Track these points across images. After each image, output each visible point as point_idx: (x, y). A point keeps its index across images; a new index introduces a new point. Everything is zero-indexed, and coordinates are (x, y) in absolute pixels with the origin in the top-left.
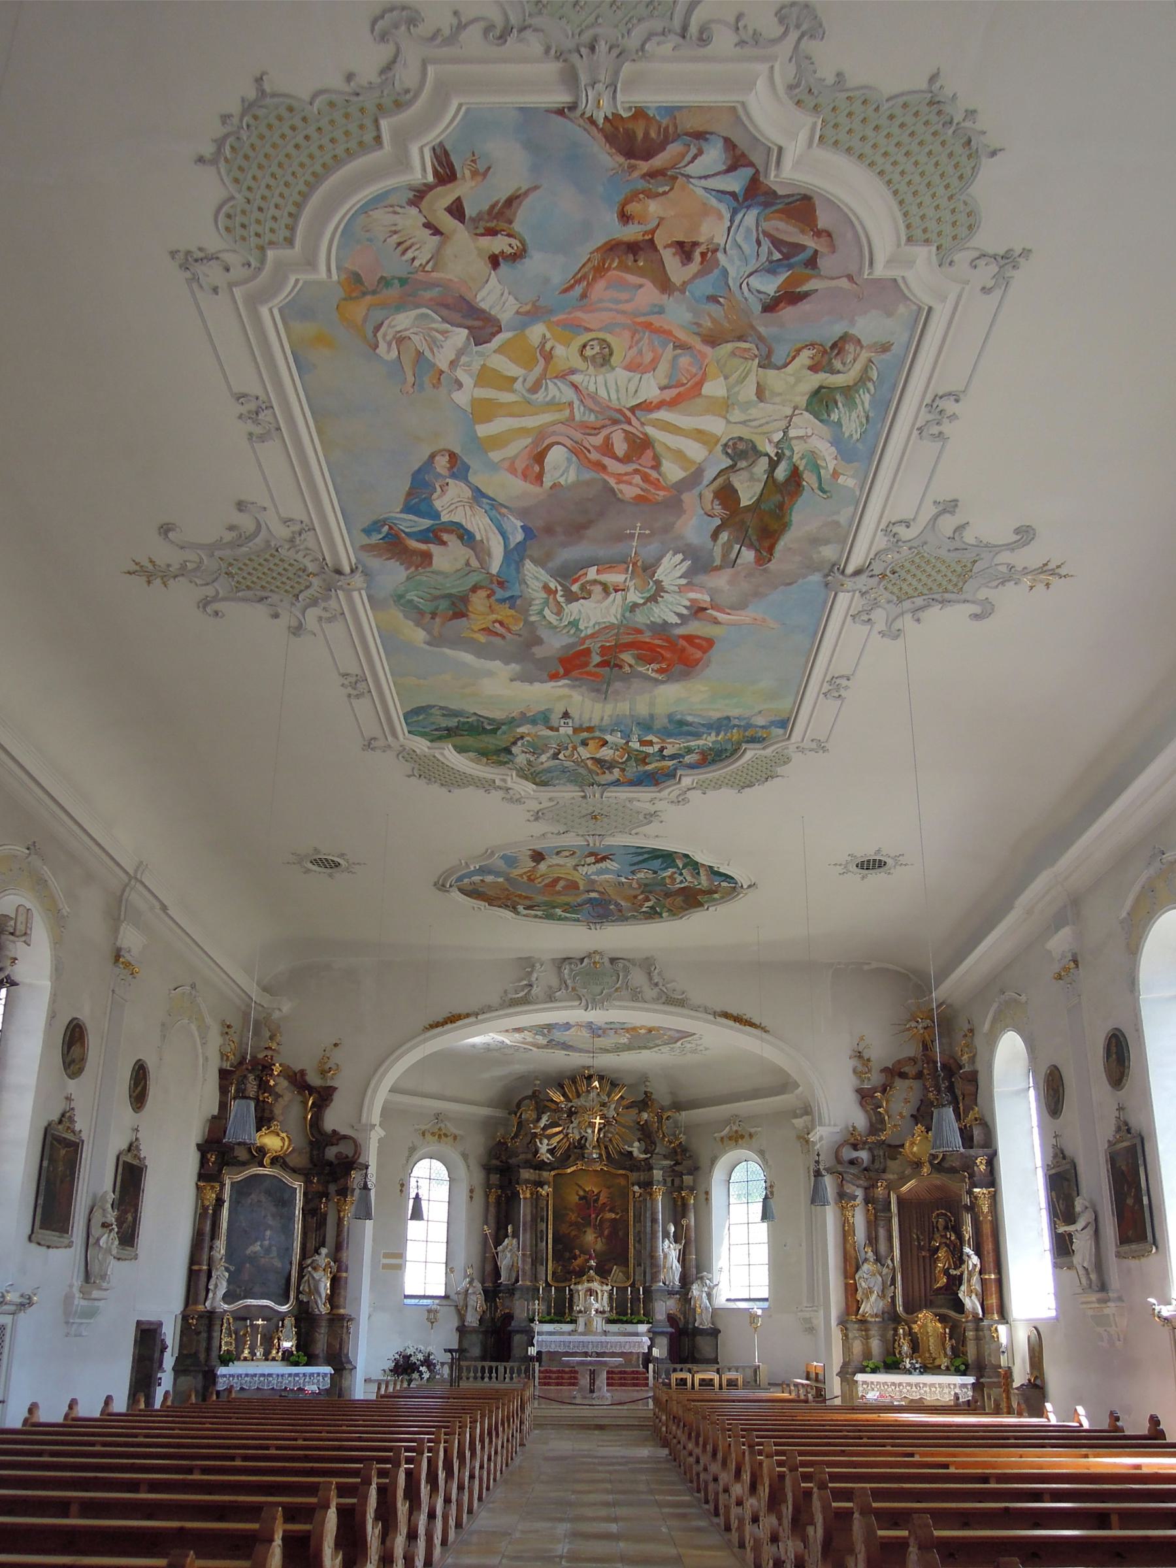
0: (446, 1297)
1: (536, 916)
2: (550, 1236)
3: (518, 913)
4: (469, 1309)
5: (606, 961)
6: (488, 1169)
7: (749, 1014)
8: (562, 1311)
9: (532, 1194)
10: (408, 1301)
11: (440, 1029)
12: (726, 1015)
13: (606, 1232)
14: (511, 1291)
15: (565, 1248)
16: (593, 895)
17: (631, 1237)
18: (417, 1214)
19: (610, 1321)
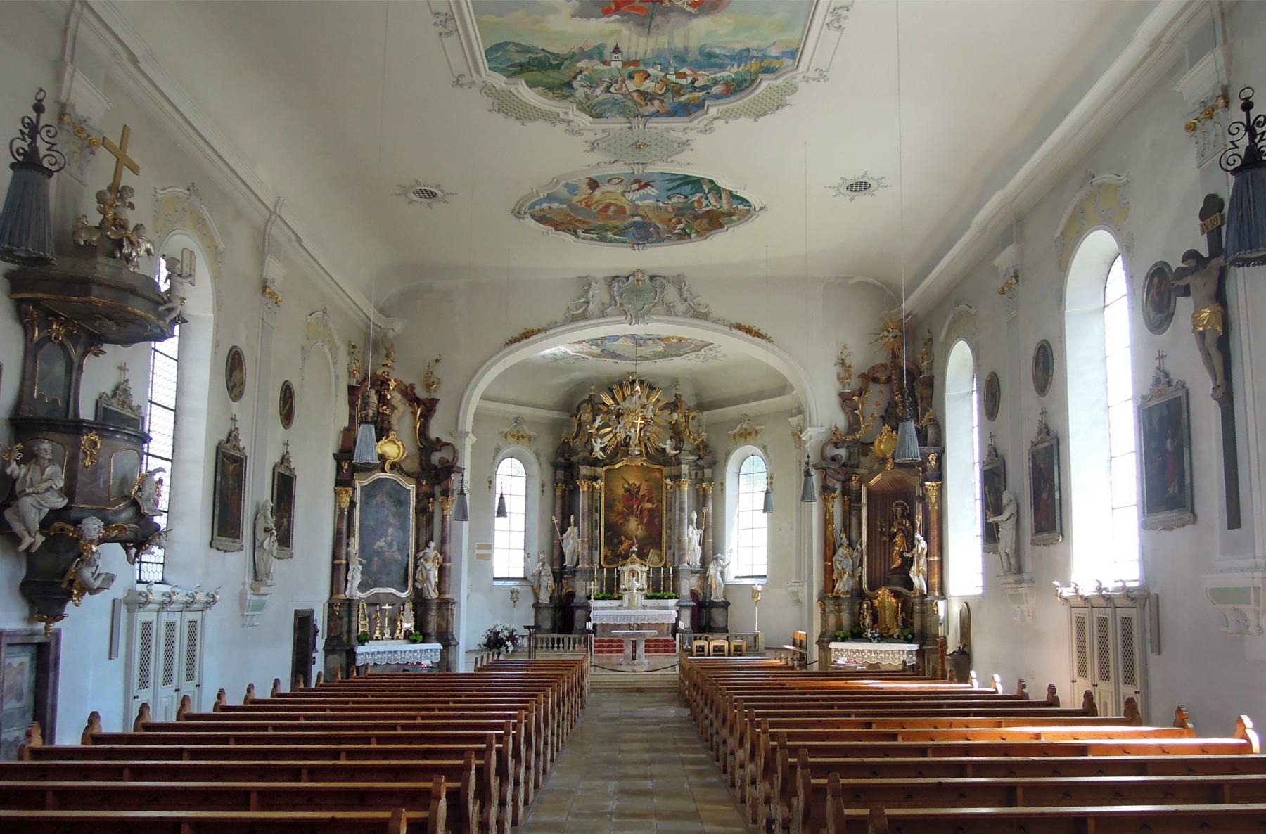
0: (525, 579)
1: (592, 239)
3: (578, 237)
5: (647, 278)
7: (759, 326)
8: (611, 590)
10: (496, 583)
11: (517, 344)
12: (739, 327)
14: (573, 573)
15: (614, 534)
16: (637, 219)
18: (502, 512)
19: (648, 597)
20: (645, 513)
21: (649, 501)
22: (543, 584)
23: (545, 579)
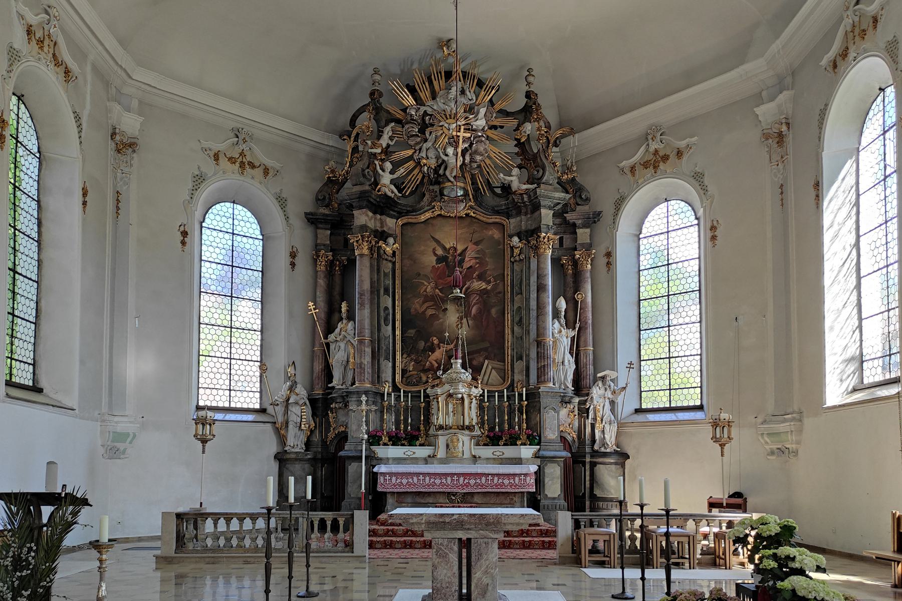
0: (262, 411)
2: (398, 316)
4: (291, 426)
6: (312, 220)
9: (371, 249)
13: (474, 310)
15: (419, 335)
17: (508, 317)
20: (474, 299)
21: (481, 278)
22: (294, 418)
23: (295, 410)
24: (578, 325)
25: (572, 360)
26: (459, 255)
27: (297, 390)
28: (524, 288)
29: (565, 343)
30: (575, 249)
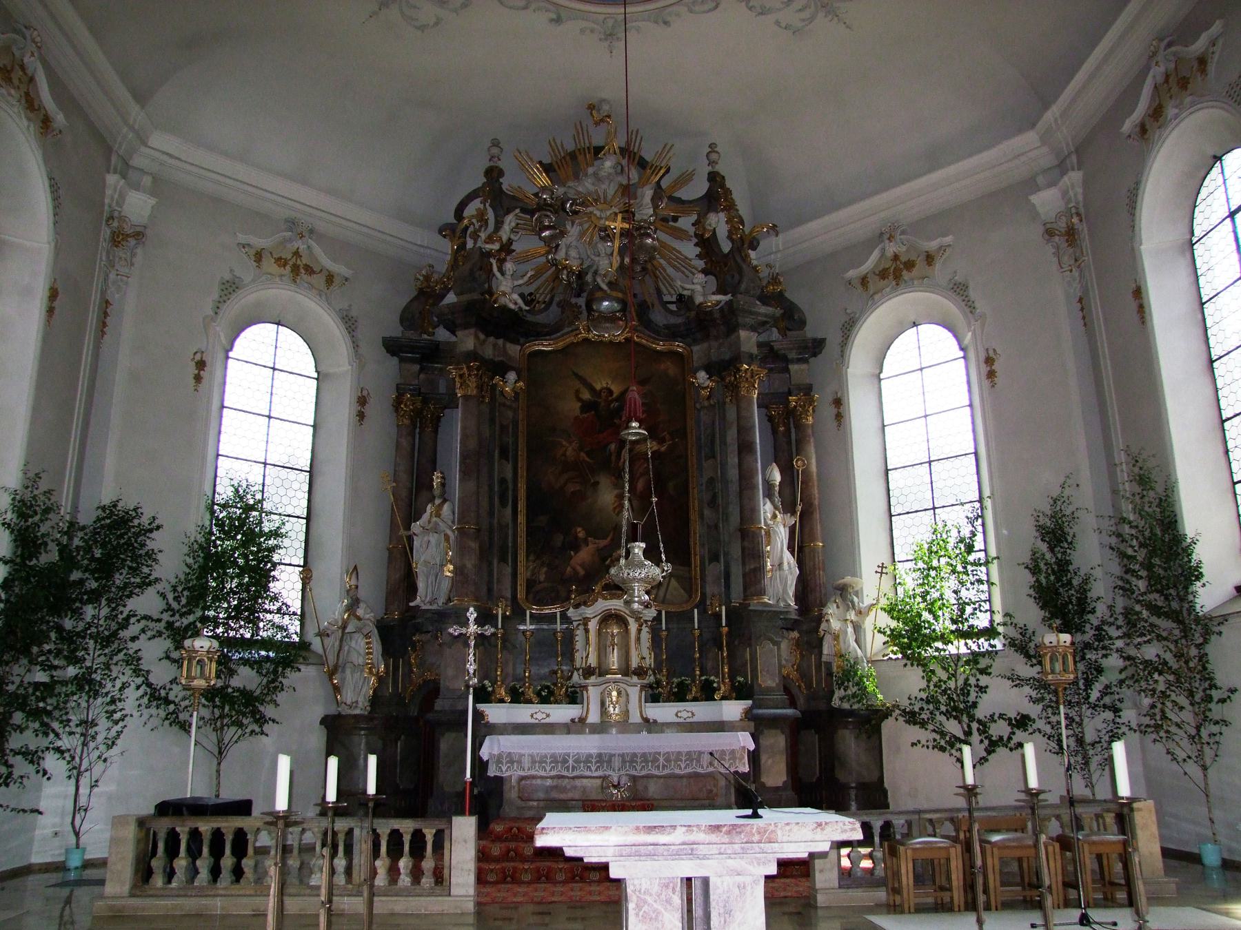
2: (522, 493)
6: (392, 347)
9: (480, 388)
23: (358, 643)
24: (799, 508)
25: (793, 561)
26: (616, 400)
27: (360, 612)
28: (717, 448)
29: (781, 535)
30: (790, 394)
